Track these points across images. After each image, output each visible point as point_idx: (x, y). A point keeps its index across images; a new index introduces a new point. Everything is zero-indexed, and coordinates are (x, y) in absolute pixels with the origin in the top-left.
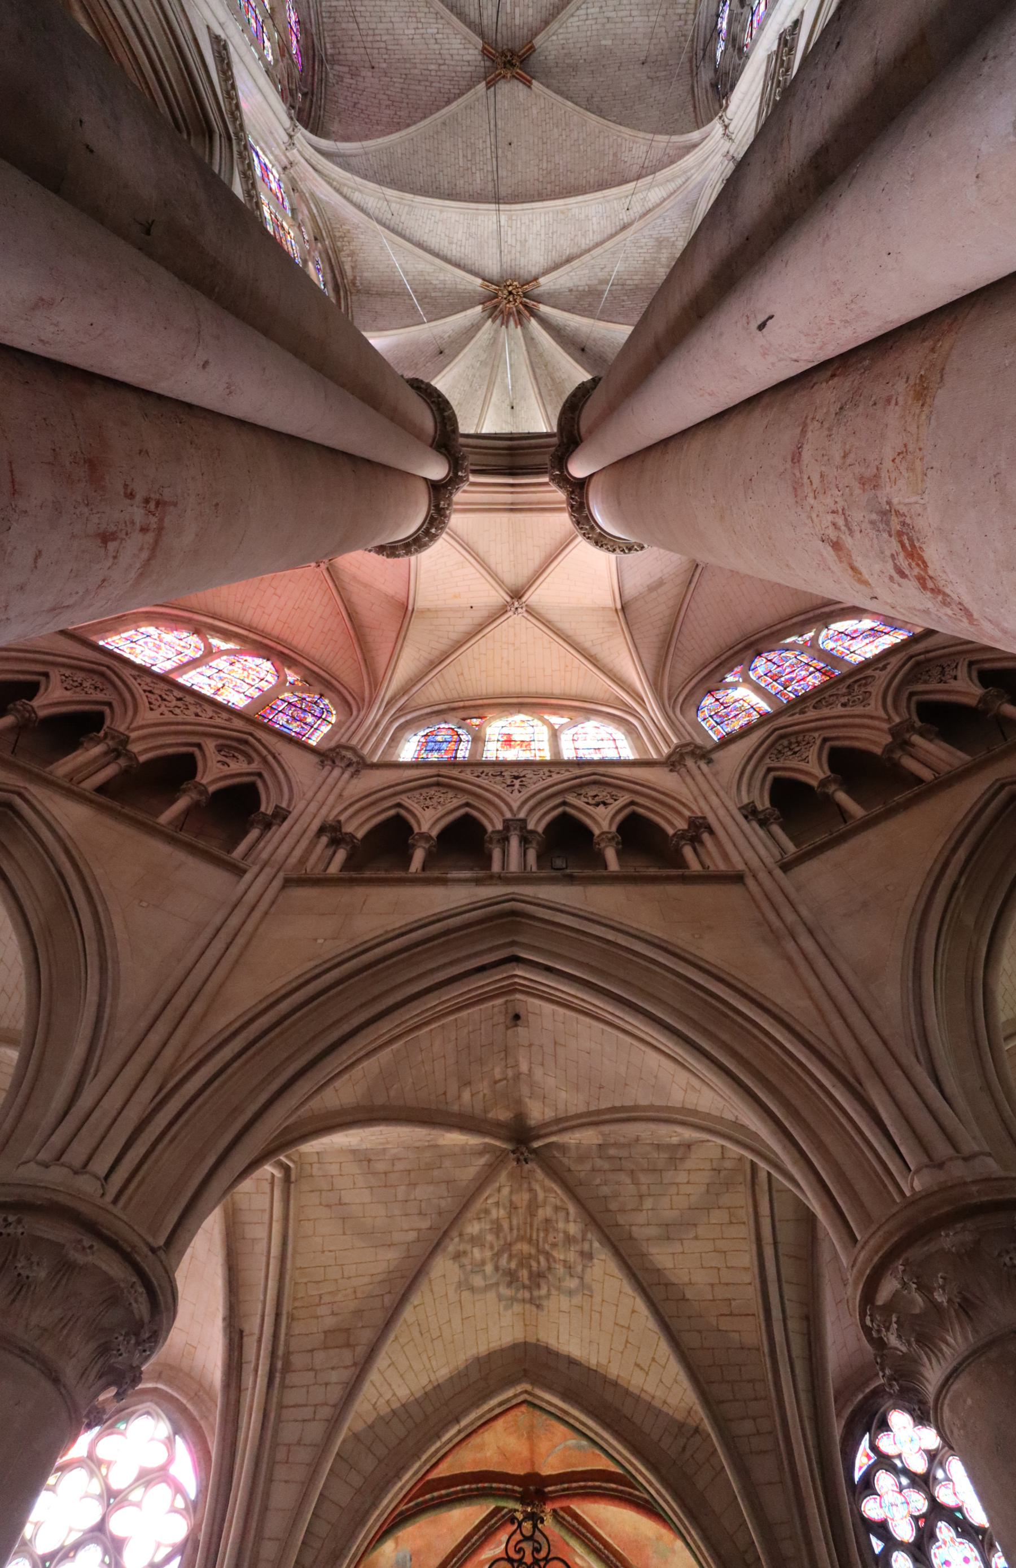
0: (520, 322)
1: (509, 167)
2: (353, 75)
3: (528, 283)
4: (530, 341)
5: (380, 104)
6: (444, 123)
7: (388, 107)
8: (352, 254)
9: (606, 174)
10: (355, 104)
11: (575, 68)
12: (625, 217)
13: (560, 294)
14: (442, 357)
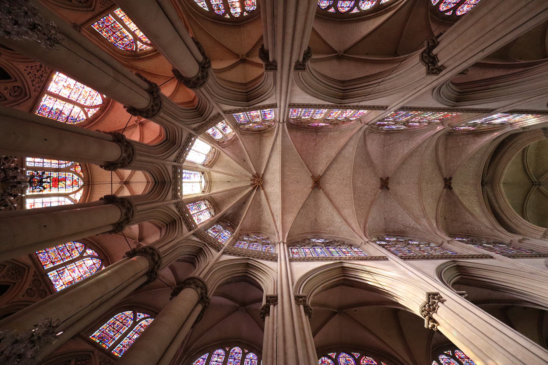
0: (252, 185)
2: (313, 139)
3: (262, 187)
4: (247, 187)
6: (302, 164)
8: (268, 136)
9: (287, 209)
10: (306, 140)
11: (316, 200)
12: (275, 216)
13: (260, 196)
14: (243, 161)
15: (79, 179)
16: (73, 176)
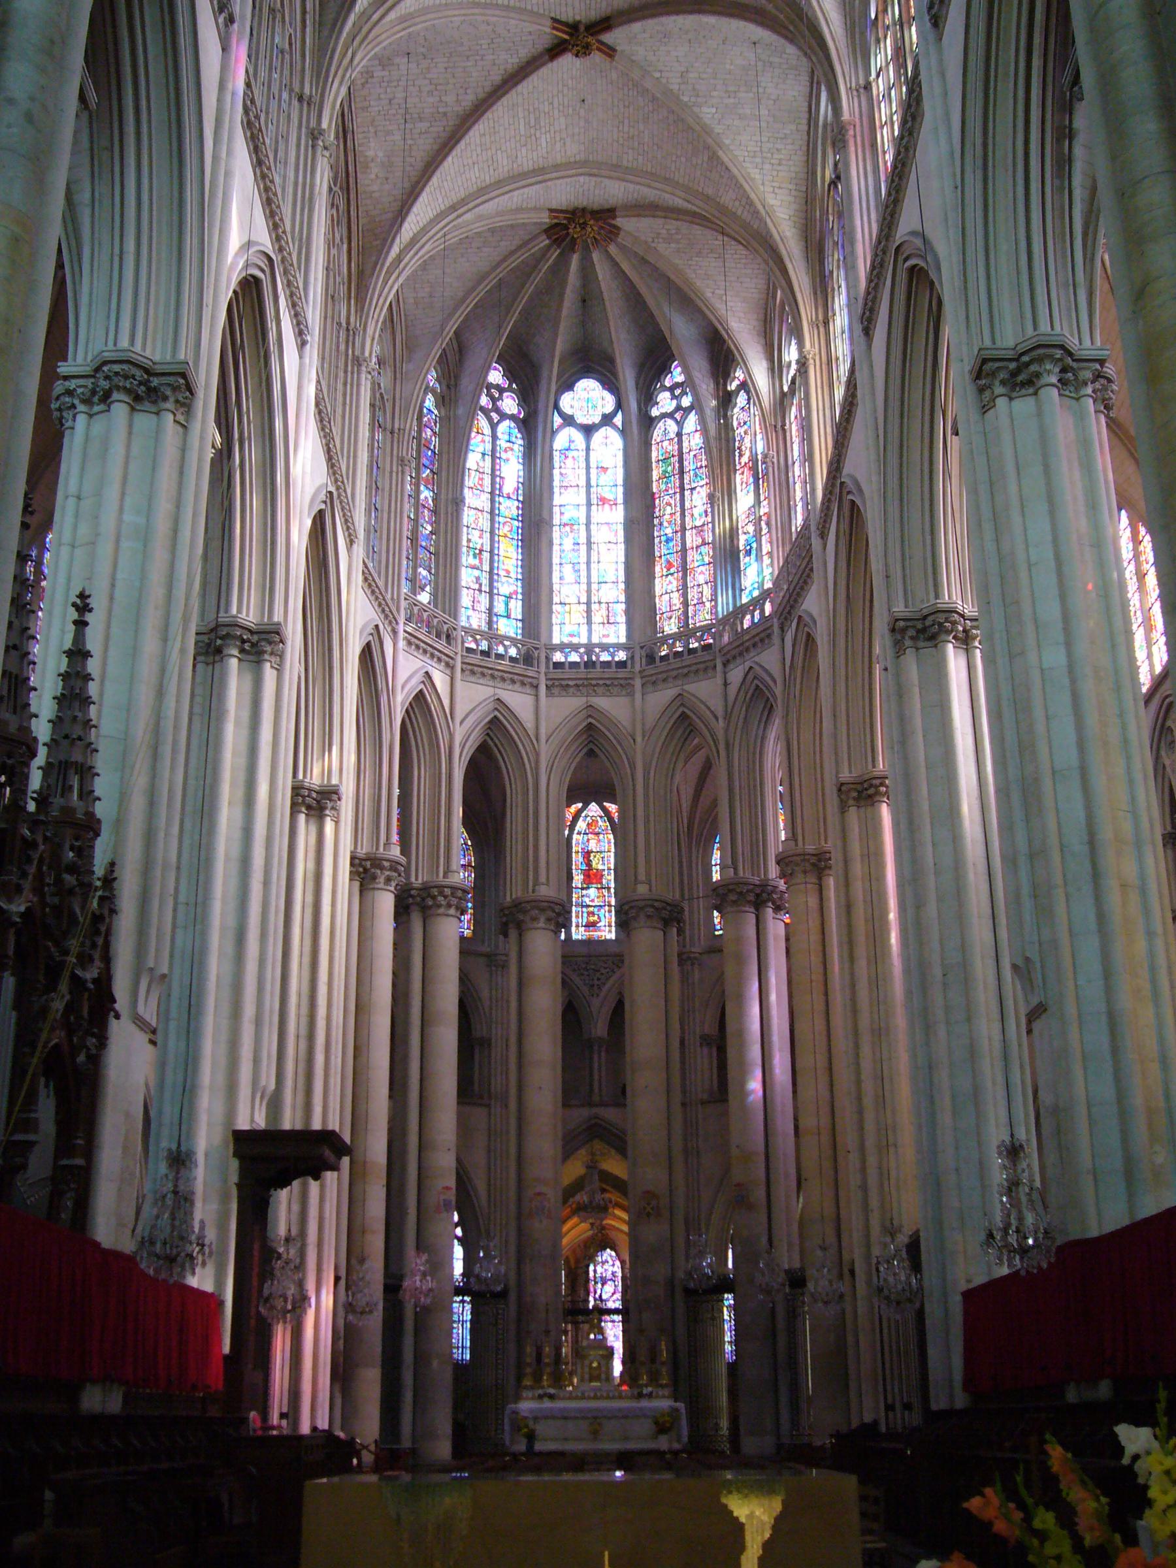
1: (582, 123)
5: (420, 91)
7: (430, 93)
15: (586, 816)
16: (579, 833)
